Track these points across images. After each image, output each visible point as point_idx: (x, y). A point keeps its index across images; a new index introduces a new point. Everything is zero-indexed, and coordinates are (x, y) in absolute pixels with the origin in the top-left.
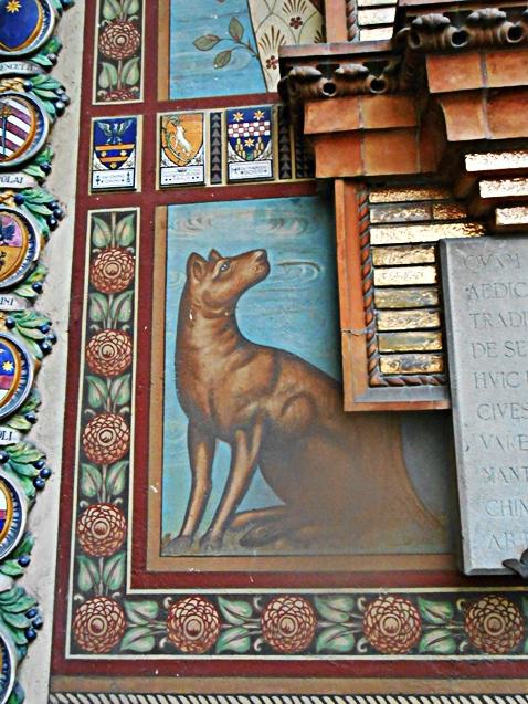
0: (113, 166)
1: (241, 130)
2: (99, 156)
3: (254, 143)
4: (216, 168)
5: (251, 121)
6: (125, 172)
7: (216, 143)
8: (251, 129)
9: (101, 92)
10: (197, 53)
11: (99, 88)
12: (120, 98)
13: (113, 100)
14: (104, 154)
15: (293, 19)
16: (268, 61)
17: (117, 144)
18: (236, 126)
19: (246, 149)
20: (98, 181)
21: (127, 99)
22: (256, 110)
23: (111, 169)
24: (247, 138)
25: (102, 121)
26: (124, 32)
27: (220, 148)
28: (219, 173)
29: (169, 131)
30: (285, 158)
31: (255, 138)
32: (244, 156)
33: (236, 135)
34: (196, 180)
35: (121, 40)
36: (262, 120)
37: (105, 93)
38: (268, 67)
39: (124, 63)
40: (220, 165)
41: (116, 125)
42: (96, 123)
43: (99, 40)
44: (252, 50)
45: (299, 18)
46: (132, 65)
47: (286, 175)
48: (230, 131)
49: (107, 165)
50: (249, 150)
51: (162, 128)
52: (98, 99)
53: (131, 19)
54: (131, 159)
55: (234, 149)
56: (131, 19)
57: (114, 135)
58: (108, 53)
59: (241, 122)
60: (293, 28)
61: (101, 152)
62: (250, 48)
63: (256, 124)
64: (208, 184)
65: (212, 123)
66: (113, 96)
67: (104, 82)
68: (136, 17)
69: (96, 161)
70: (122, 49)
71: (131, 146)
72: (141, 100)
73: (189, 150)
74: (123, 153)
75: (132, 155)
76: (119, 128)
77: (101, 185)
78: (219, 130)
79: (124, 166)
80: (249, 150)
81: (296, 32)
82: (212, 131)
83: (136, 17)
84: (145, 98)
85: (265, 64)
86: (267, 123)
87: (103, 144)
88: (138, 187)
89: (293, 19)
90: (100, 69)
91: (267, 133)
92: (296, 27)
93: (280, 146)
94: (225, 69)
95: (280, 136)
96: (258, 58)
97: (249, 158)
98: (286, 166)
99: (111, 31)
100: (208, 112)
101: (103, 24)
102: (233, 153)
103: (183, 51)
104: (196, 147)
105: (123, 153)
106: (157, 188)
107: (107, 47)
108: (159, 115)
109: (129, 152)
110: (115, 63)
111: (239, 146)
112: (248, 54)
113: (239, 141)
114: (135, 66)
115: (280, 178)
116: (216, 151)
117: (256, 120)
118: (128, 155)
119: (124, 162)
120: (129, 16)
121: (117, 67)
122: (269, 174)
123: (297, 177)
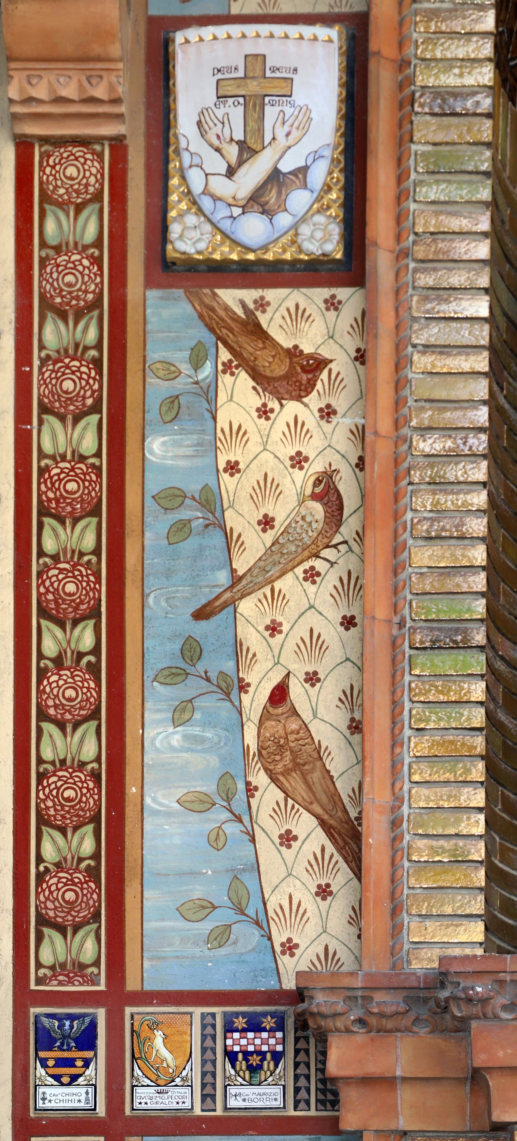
0: (66, 1080)
1: (244, 1042)
2: (44, 1065)
3: (262, 1061)
4: (208, 1090)
5: (257, 1028)
6: (83, 1090)
7: (209, 1055)
8: (258, 1042)
9: (42, 972)
10: (181, 924)
11: (39, 965)
12: (70, 982)
13: (60, 983)
14: (51, 1063)
15: (319, 886)
16: (283, 945)
17: (69, 1049)
18: (236, 1035)
19: (250, 1067)
20: (44, 1099)
21: (81, 984)
22: (265, 1014)
23: (63, 1085)
24: (251, 1053)
25: (49, 1016)
26: (75, 884)
27: (214, 1062)
28: (213, 1097)
29: (143, 1035)
30: (302, 1082)
31: (263, 1054)
32: (247, 1077)
33: (237, 1048)
34: (181, 1106)
35: (70, 896)
36: (272, 1030)
37: (49, 973)
38: (283, 953)
39: (76, 930)
40: (214, 1085)
41: (68, 1023)
42: (36, 1017)
43: (37, 894)
44: (261, 927)
45: (328, 885)
46: (87, 934)
47: (302, 1105)
48: (229, 1042)
49: (57, 1078)
50: (253, 1069)
51: (133, 1031)
52: (39, 981)
53: (83, 865)
54: (90, 1072)
55: (234, 1067)
56: (83, 865)
57: (64, 1037)
58: (51, 914)
59: (244, 1030)
60: (318, 899)
61: (47, 1059)
62: (257, 923)
63: (265, 1035)
64: (198, 1111)
65: (204, 1027)
66: (61, 978)
67: (47, 957)
68: (92, 863)
69: (41, 1071)
70: (72, 909)
71: (89, 1054)
72: (102, 987)
73: (171, 1063)
74: (79, 1063)
75: (92, 1066)
76: (71, 1027)
77: (48, 1105)
78: (214, 1037)
79: (81, 1080)
80: (253, 1069)
81: (324, 905)
82: (204, 1037)
83: (92, 863)
84: (107, 985)
85: (278, 949)
86: (279, 1035)
87: (50, 1049)
88: (101, 1111)
89: (319, 886)
90: (39, 938)
91: (279, 1048)
92: (324, 899)
93: (296, 1065)
94: (223, 951)
95: (297, 1052)
96: (270, 939)
97: (255, 1080)
98: (303, 1094)
99: (55, 880)
100: (198, 1011)
101: (41, 868)
102: (233, 1072)
103: (163, 920)
104: (181, 1061)
105: (79, 1063)
106: (128, 1112)
107: (50, 905)
108: (128, 1010)
109: (87, 1064)
110: (62, 930)
111: (241, 1064)
112: (256, 932)
113: (240, 1056)
114: (93, 934)
115: (295, 1110)
116: (209, 1067)
117: (264, 1030)
118: (87, 1065)
119: (81, 1075)
120: (81, 860)
121: (65, 937)
122: (279, 1103)
123: (317, 1110)
